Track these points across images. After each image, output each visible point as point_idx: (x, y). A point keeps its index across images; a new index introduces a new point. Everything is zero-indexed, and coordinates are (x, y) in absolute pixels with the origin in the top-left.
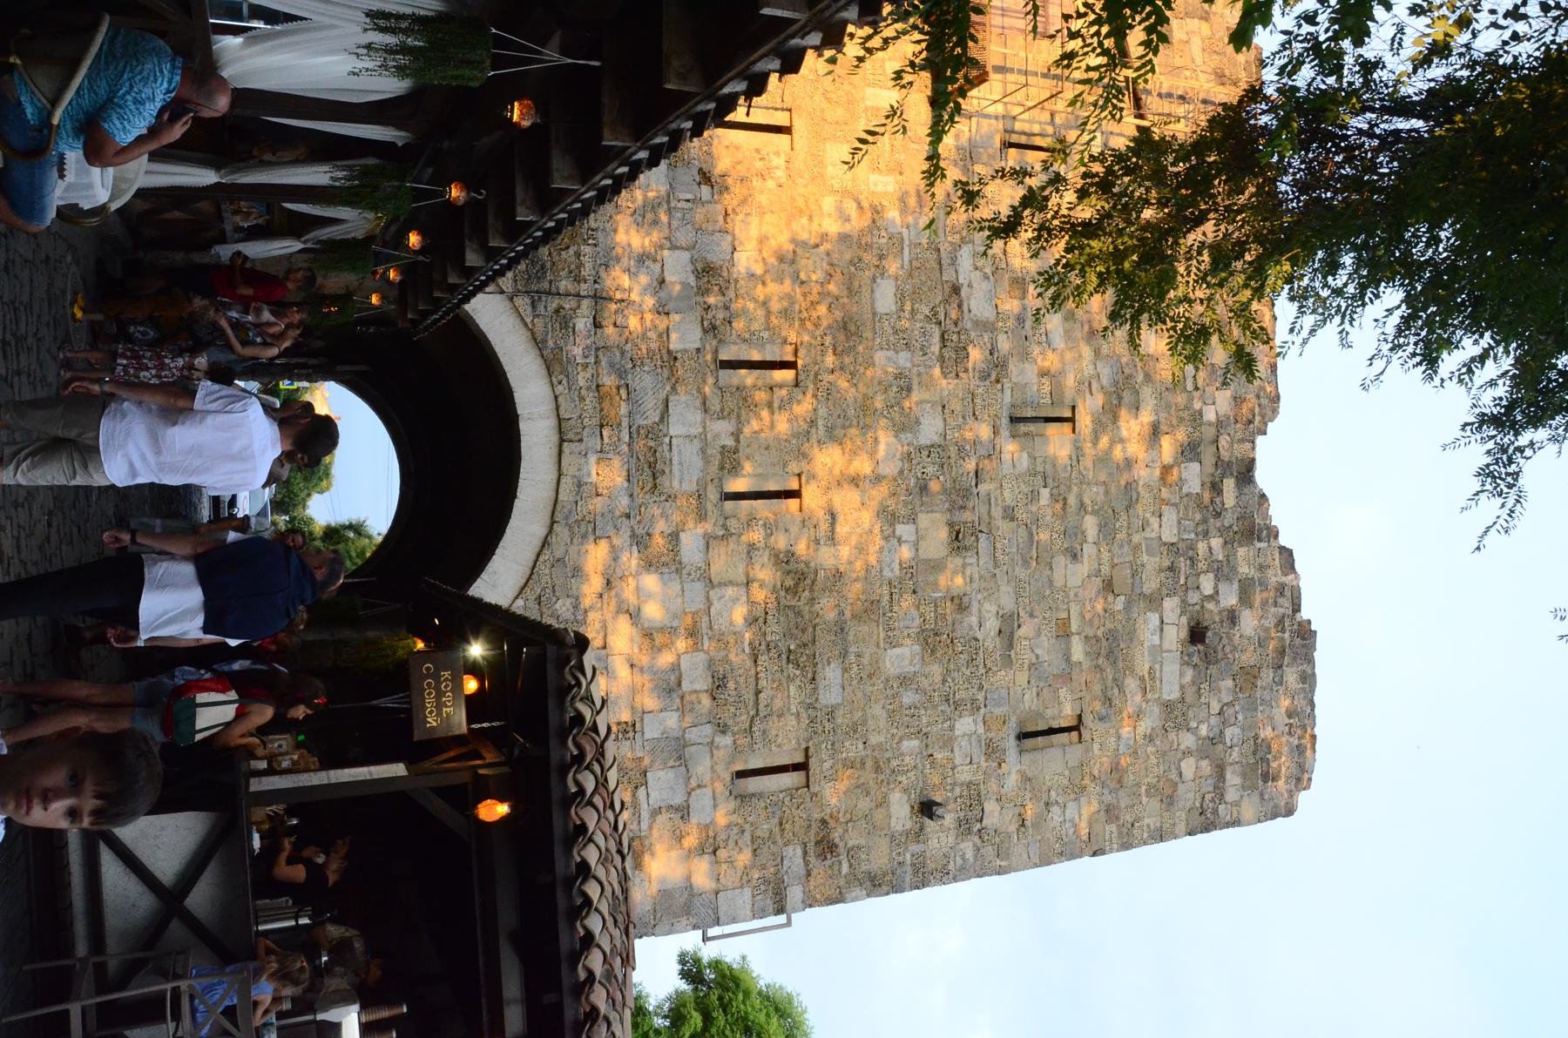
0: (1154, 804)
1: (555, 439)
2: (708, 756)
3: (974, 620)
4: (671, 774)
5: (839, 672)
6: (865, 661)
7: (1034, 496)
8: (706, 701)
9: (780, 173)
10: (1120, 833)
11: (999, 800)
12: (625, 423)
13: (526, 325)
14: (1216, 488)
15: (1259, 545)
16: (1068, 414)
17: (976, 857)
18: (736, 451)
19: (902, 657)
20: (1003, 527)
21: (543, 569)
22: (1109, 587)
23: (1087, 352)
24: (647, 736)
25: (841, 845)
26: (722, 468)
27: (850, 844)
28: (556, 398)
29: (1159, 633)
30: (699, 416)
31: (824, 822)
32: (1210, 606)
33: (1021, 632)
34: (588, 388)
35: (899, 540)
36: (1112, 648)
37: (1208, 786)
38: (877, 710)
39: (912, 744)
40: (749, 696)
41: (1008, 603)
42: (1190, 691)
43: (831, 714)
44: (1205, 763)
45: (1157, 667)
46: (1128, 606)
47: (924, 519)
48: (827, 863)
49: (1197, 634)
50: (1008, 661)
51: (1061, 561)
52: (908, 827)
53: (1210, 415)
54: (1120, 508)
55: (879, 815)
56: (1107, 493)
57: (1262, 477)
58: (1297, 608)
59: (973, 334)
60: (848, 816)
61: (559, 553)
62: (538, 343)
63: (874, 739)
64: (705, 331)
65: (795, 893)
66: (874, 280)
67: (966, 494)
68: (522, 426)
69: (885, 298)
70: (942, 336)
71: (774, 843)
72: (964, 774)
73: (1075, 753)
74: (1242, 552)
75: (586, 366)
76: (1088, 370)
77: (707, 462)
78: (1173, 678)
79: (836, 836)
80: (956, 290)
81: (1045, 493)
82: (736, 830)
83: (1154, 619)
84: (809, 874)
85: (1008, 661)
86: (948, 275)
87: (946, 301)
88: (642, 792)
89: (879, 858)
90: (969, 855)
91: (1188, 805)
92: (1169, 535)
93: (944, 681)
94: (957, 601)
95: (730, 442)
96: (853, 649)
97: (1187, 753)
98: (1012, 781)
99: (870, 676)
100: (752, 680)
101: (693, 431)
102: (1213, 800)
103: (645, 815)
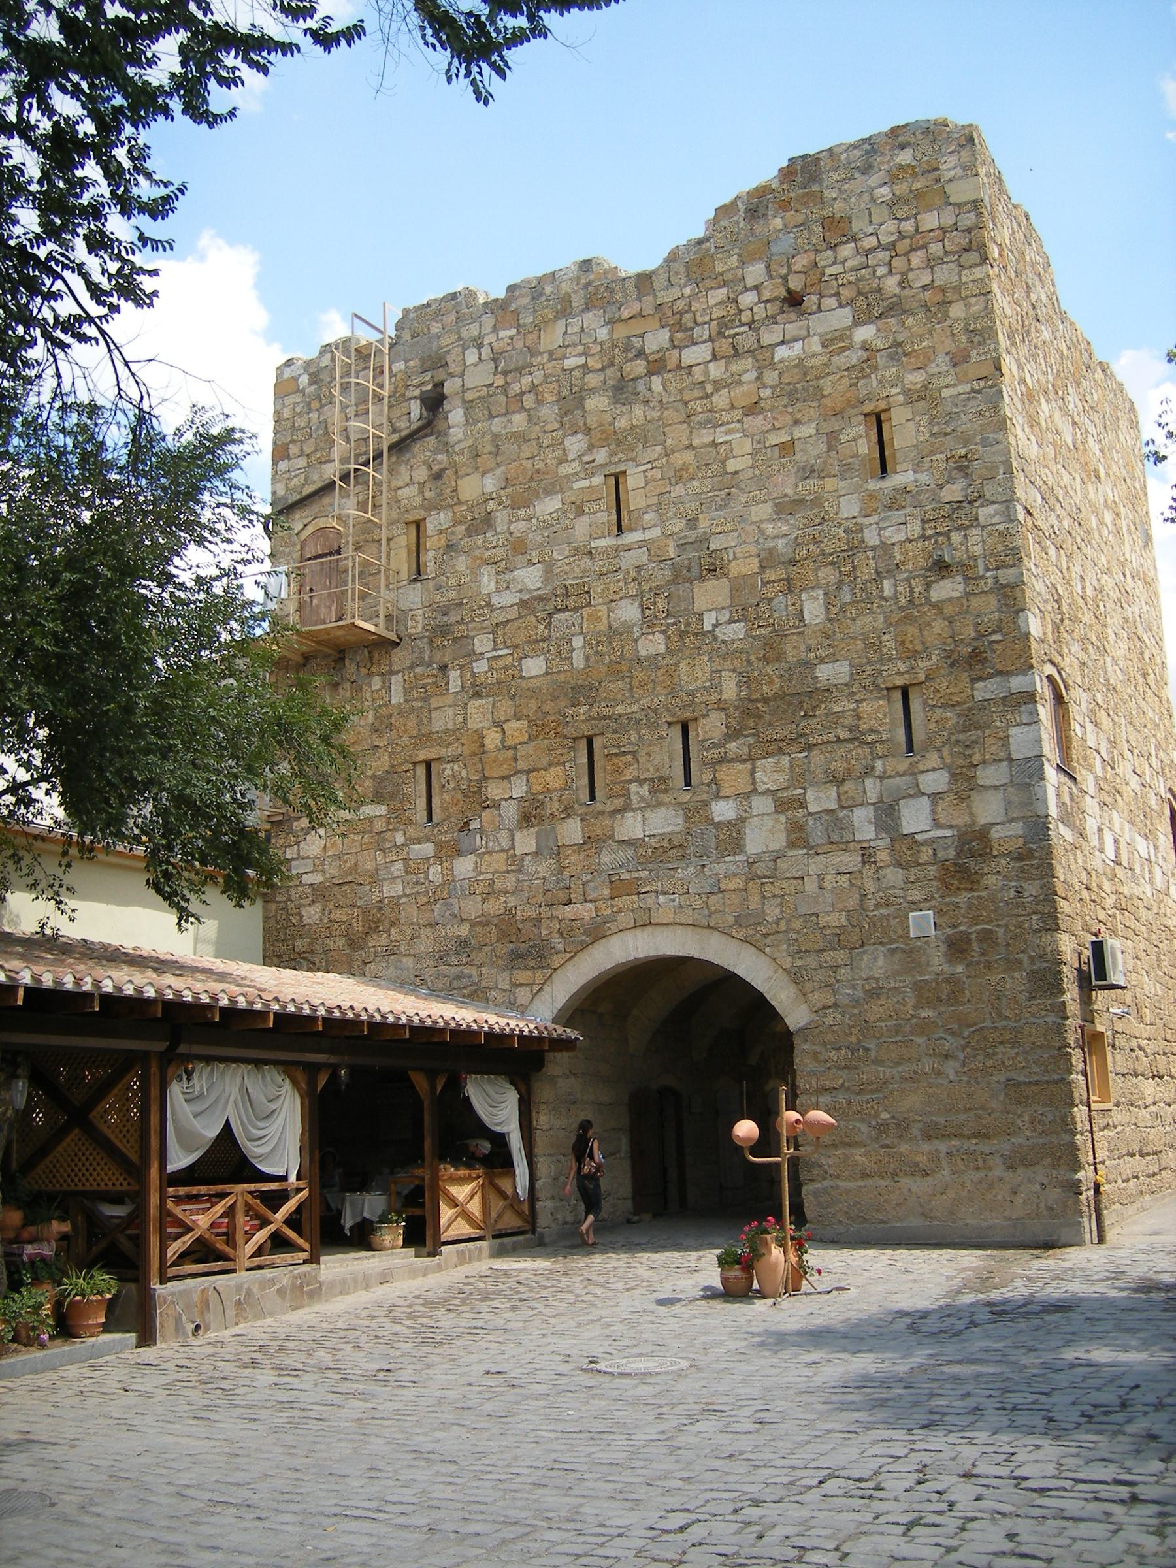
1: (650, 929)
2: (891, 780)
3: (781, 543)
6: (813, 642)
8: (849, 786)
10: (979, 343)
11: (941, 487)
22: (752, 409)
23: (564, 470)
24: (873, 836)
26: (666, 791)
27: (973, 635)
31: (952, 665)
33: (790, 491)
39: (887, 587)
41: (767, 509)
43: (856, 670)
47: (699, 605)
49: (794, 301)
50: (817, 502)
52: (959, 578)
53: (603, 334)
55: (949, 610)
59: (556, 583)
60: (949, 640)
61: (731, 920)
62: (584, 947)
63: (880, 622)
64: (569, 816)
65: (1017, 683)
66: (522, 677)
68: (641, 956)
69: (534, 667)
70: (559, 611)
71: (970, 709)
72: (915, 528)
73: (899, 416)
76: (575, 467)
77: (660, 804)
80: (523, 604)
83: (782, 352)
84: (1000, 673)
85: (817, 502)
88: (918, 837)
90: (991, 509)
93: (832, 563)
95: (646, 787)
101: (639, 818)
103: (939, 833)
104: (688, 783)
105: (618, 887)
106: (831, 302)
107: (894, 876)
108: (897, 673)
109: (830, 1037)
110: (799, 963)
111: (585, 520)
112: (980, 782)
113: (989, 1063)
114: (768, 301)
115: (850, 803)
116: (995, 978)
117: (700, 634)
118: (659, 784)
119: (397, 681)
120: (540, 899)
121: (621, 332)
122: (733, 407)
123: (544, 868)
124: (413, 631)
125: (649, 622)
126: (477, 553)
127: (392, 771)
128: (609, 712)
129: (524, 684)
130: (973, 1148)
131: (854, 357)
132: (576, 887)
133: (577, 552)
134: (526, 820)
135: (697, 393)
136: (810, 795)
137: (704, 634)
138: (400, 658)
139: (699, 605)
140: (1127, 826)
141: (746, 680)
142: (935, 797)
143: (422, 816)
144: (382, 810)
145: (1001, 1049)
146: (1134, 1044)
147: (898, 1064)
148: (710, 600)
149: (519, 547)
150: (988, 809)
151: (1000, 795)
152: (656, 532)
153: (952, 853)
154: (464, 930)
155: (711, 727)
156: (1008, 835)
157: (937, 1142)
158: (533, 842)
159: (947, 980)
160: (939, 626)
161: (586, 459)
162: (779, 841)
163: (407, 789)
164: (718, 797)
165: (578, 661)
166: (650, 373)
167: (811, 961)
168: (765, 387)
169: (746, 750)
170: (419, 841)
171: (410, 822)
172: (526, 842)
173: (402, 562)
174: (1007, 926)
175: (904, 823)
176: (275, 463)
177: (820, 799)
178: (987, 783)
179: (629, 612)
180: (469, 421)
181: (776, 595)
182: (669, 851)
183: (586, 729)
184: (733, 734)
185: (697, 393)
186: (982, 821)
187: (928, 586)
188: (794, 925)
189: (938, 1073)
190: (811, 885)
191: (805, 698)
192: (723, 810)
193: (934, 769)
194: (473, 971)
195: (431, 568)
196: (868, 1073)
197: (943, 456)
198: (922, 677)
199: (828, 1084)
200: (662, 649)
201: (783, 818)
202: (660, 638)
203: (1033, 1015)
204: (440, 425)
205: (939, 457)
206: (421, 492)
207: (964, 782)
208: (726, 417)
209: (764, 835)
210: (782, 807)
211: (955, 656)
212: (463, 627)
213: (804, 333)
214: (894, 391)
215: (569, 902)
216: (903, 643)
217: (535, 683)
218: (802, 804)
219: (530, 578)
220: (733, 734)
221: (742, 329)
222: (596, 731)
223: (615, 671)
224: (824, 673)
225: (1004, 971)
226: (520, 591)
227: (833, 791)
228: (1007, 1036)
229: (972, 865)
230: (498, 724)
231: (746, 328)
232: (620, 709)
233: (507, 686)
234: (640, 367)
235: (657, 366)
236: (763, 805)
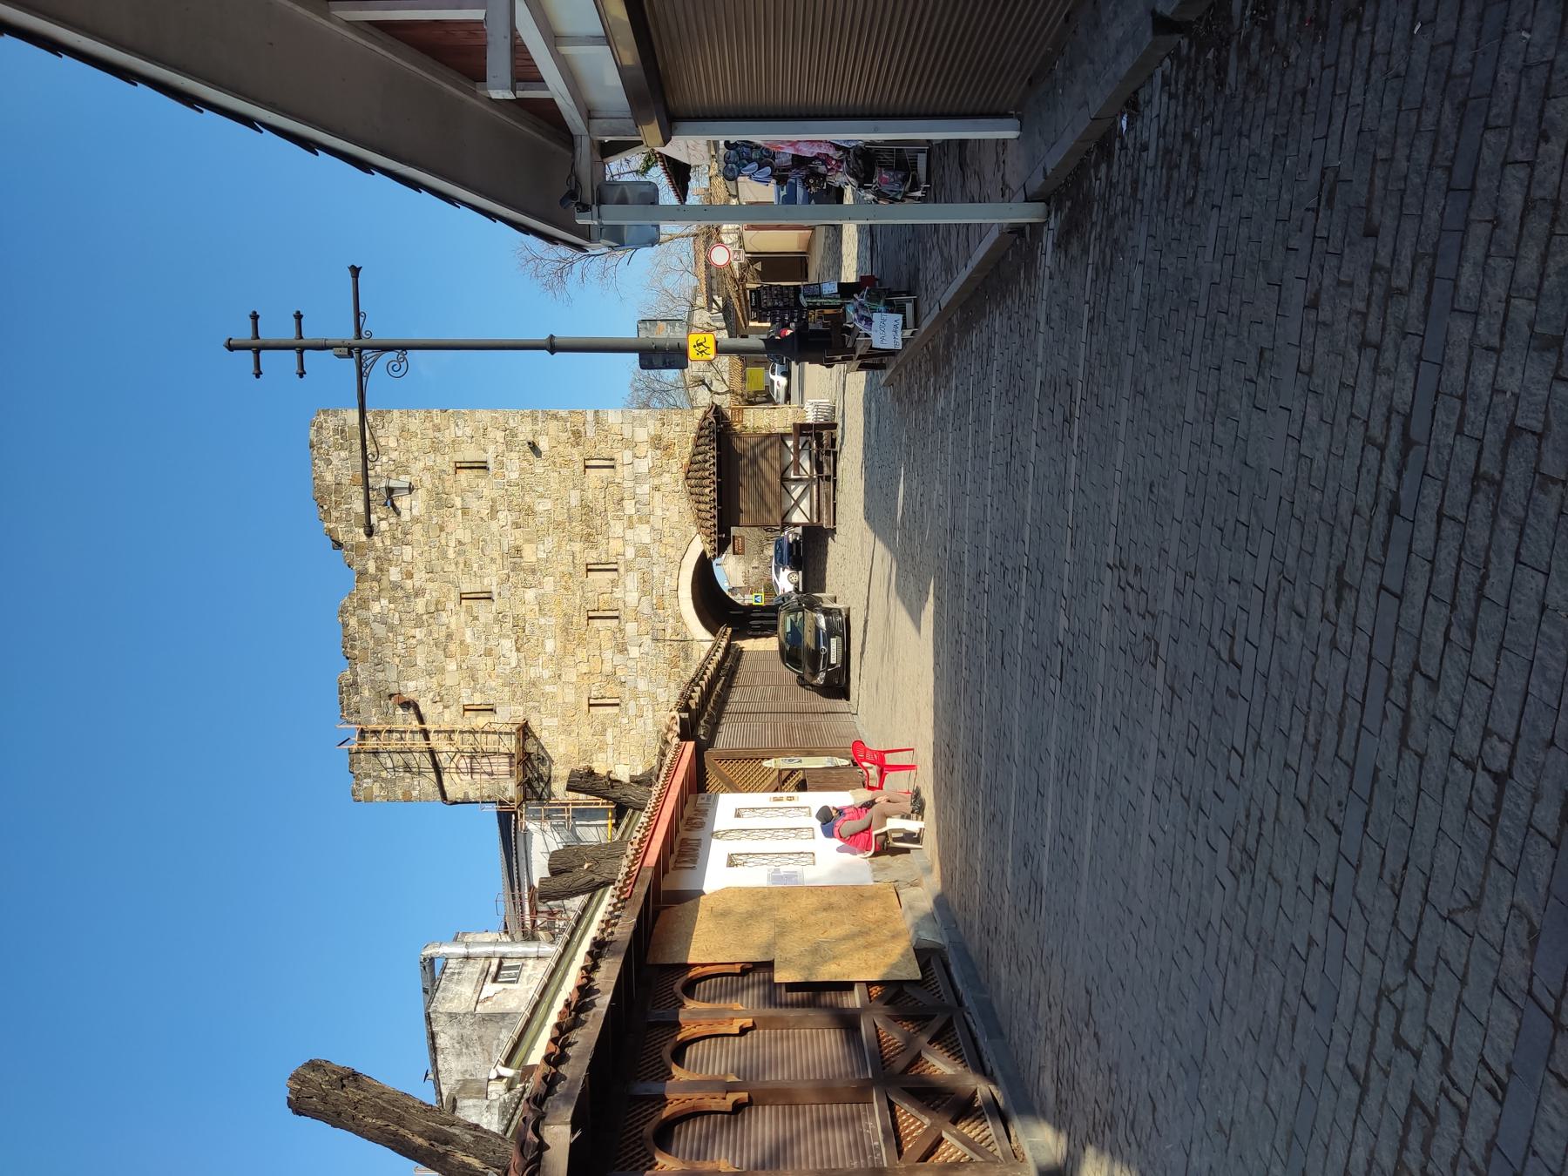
0: (413, 429)
19: (543, 506)
20: (496, 555)
22: (442, 529)
23: (453, 626)
36: (440, 501)
43: (574, 487)
46: (431, 518)
47: (534, 559)
50: (494, 501)
51: (467, 539)
53: (384, 602)
69: (550, 645)
72: (513, 455)
76: (453, 619)
80: (518, 650)
81: (475, 566)
85: (494, 501)
89: (553, 426)
92: (407, 550)
98: (491, 448)
107: (666, 478)
127: (591, 724)
139: (534, 559)
148: (530, 555)
150: (642, 435)
155: (592, 557)
160: (560, 448)
162: (646, 528)
172: (634, 652)
177: (629, 507)
179: (530, 595)
184: (594, 546)
186: (646, 438)
207: (630, 444)
209: (643, 534)
218: (630, 517)
219: (507, 644)
220: (594, 546)
233: (558, 660)
235: (410, 576)
236: (629, 534)
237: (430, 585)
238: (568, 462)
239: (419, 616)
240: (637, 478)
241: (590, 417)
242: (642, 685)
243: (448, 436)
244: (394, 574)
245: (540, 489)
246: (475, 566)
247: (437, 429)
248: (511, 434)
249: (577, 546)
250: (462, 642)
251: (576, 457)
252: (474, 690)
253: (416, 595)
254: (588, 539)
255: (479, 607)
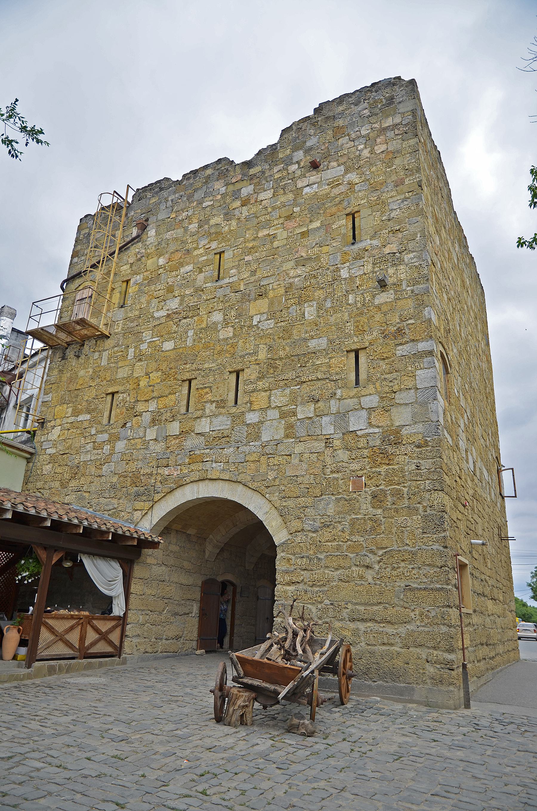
0: (397, 161)
2: (345, 401)
4: (352, 419)
5: (313, 341)
7: (248, 263)
8: (320, 404)
9: (125, 396)
10: (410, 175)
11: (385, 246)
12: (203, 451)
13: (165, 496)
14: (252, 178)
15: (279, 148)
16: (218, 256)
17: (413, 252)
18: (217, 401)
19: (310, 312)
20: (259, 275)
21: (255, 485)
22: (289, 217)
23: (196, 253)
25: (398, 325)
26: (224, 407)
27: (398, 321)
28: (192, 482)
29: (311, 185)
30: (203, 419)
32: (302, 164)
33: (304, 254)
34: (189, 468)
35: (259, 322)
37: (390, 134)
38: (332, 319)
40: (320, 383)
41: (292, 263)
42: (342, 160)
43: (331, 341)
44: (378, 140)
45: (327, 182)
48: (407, 331)
49: (315, 166)
51: (276, 244)
54: (255, 221)
55: (384, 308)
56: (248, 229)
57: (249, 156)
58: (308, 118)
61: (249, 478)
63: (346, 317)
64: (174, 420)
66: (162, 351)
67: (244, 295)
69: (168, 346)
70: (185, 318)
72: (369, 268)
73: (364, 212)
74: (281, 156)
75: (181, 470)
76: (202, 251)
77: (220, 414)
78: (334, 171)
79: (393, 329)
80: (168, 316)
81: (247, 258)
82: (384, 383)
83: (307, 190)
85: (318, 258)
86: (163, 320)
87: (172, 320)
88: (359, 433)
90: (412, 255)
91: (400, 141)
92: (269, 194)
93: (323, 288)
94: (287, 290)
95: (214, 405)
96: (303, 336)
97: (372, 152)
99: (316, 325)
100: (312, 383)
102: (399, 129)
103: (371, 430)
104: (236, 403)
105: (194, 459)
106: (334, 164)
107: (343, 455)
108: (354, 343)
109: (298, 550)
110: (284, 504)
111: (203, 274)
112: (398, 402)
113: (395, 573)
114: (302, 167)
115: (321, 413)
116: (401, 519)
117: (251, 326)
118: (221, 404)
119: (105, 354)
120: (154, 463)
121: (231, 188)
122: (280, 217)
123: (159, 447)
124: (116, 331)
125: (226, 323)
126: (151, 293)
128: (200, 367)
129: (163, 354)
130: (381, 629)
131: (342, 188)
132: (172, 458)
133: (197, 290)
134: (154, 422)
135: (264, 212)
136: (299, 409)
137: (253, 327)
138: (109, 343)
140: (479, 460)
141: (270, 348)
142: (371, 410)
143: (105, 421)
144: (88, 417)
145: (402, 564)
146: (483, 578)
147: (337, 569)
148: (257, 310)
149: (170, 290)
150: (401, 417)
151: (409, 409)
152: (235, 279)
153: (378, 442)
154: (115, 480)
156: (413, 431)
157: (358, 623)
158: (155, 434)
159: (370, 519)
161: (207, 247)
162: (281, 434)
163: (101, 407)
164: (251, 410)
165: (189, 343)
166: (242, 206)
167: (290, 503)
168: (296, 206)
169: (267, 384)
170: (102, 432)
171: (100, 423)
172: (151, 434)
173: (116, 298)
174: (409, 487)
175: (351, 424)
176: (72, 257)
177: (305, 411)
178: (402, 402)
179: (217, 317)
180: (158, 233)
181: (292, 305)
182: (220, 439)
183: (187, 376)
185: (264, 212)
187: (374, 296)
188: (283, 482)
189: (362, 577)
190: (295, 461)
191: (303, 358)
192: (252, 418)
193: (370, 394)
194: (115, 501)
195: (129, 302)
196: (318, 574)
197: (387, 231)
198: (367, 344)
199: (294, 579)
200: (231, 335)
201: (283, 422)
202: (231, 329)
203: (424, 544)
204: (144, 236)
205: (384, 231)
206: (131, 267)
208: (276, 222)
210: (283, 415)
211: (387, 332)
212: (139, 328)
213: (319, 180)
214: (362, 202)
215: (167, 466)
216: (358, 326)
217: (168, 354)
218: (294, 414)
219: (174, 304)
221: (289, 182)
222: (193, 377)
223: (206, 347)
224: (313, 344)
225: (406, 516)
226: (168, 310)
227: (312, 407)
228: (407, 556)
229: (390, 449)
230: (147, 374)
231: (291, 181)
232: (206, 366)
233: (156, 355)
234: (238, 203)
236: (273, 414)
237: (234, 223)
238: (360, 331)
239: (207, 221)
240: (342, 416)
241: (422, 346)
242: (120, 446)
243: (390, 194)
244: (247, 190)
245: (328, 304)
246: (247, 258)
247: (398, 184)
248: (395, 259)
249: (262, 355)
250: (182, 265)
251: (368, 338)
252: (141, 284)
253: (226, 214)
254: (271, 364)
255: (211, 271)
